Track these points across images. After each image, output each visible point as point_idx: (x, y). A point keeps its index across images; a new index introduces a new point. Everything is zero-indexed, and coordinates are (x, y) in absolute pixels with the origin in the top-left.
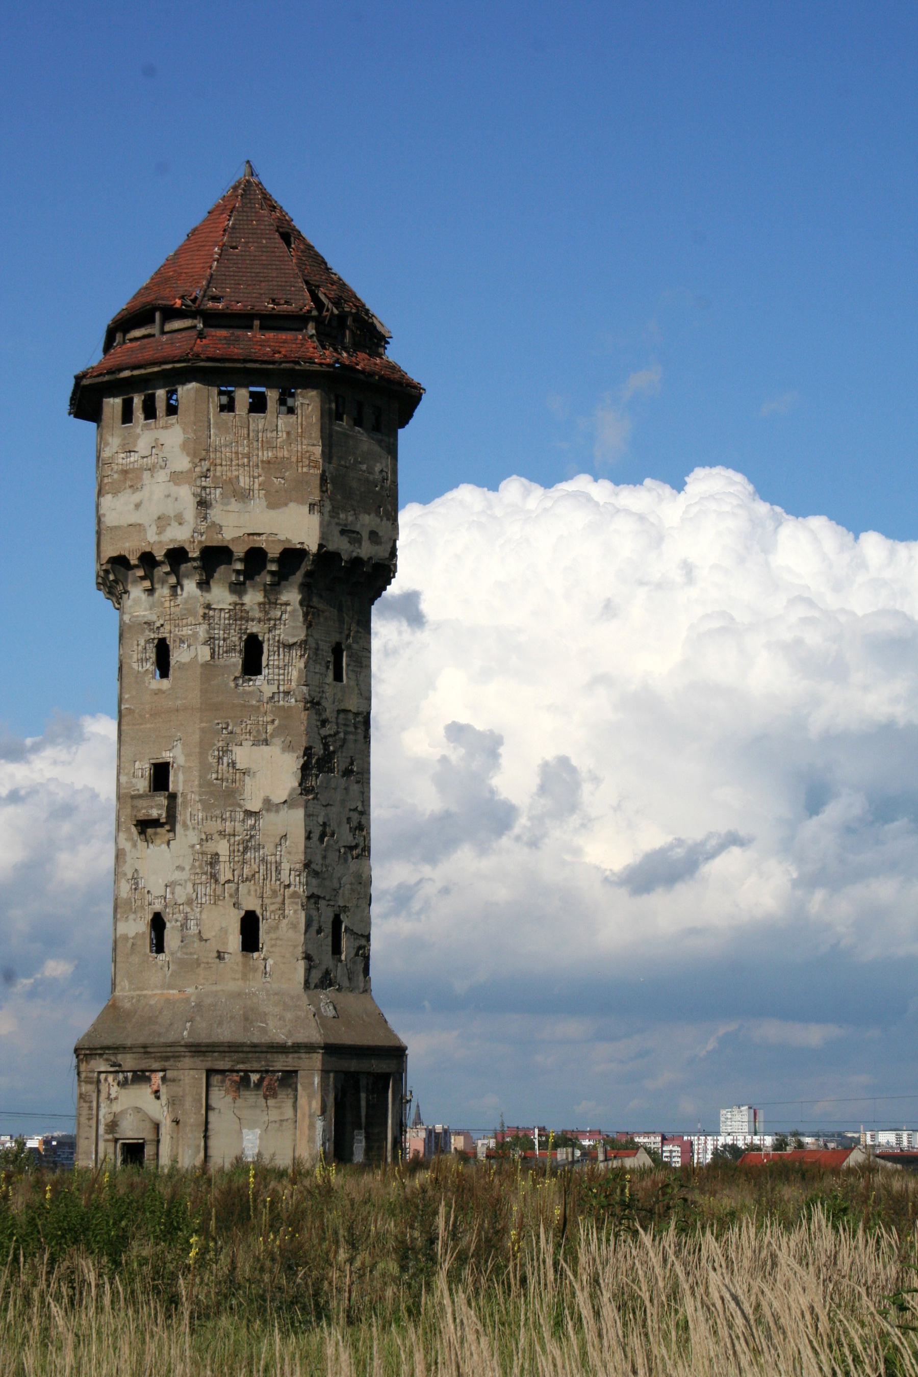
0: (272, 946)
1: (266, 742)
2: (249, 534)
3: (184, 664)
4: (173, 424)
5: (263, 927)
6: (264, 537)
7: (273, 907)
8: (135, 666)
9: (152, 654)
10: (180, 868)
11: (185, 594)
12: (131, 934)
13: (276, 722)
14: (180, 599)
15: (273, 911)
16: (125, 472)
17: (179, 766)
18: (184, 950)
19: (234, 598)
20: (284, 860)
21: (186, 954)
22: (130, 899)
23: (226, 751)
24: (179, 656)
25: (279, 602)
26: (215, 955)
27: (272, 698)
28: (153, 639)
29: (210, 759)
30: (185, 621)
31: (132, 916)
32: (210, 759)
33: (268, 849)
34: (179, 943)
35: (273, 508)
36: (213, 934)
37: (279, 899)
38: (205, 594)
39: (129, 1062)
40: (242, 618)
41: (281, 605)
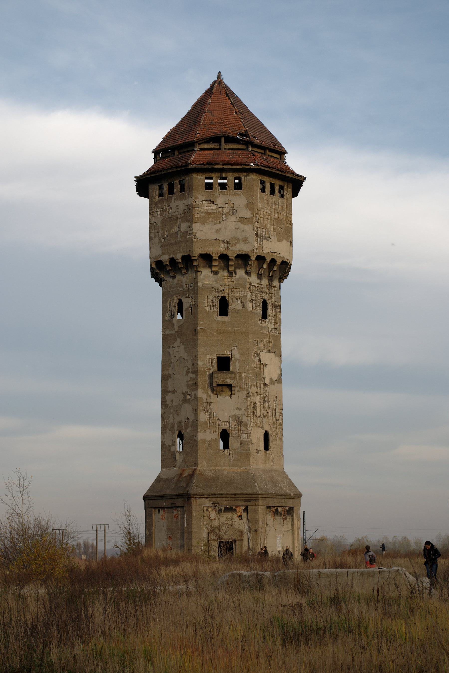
0: (274, 448)
1: (269, 351)
2: (271, 252)
4: (239, 194)
5: (271, 438)
6: (276, 254)
7: (274, 430)
8: (206, 308)
9: (217, 303)
11: (238, 276)
12: (208, 439)
13: (273, 342)
14: (234, 279)
15: (274, 432)
16: (209, 214)
17: (236, 360)
18: (242, 448)
19: (258, 281)
20: (277, 408)
21: (244, 450)
22: (206, 422)
23: (257, 354)
25: (273, 285)
26: (256, 451)
27: (271, 330)
28: (218, 296)
29: (252, 357)
30: (238, 290)
31: (208, 431)
32: (252, 357)
33: (272, 402)
34: (239, 445)
35: (279, 241)
36: (255, 441)
37: (275, 426)
38: (249, 278)
39: (224, 502)
40: (261, 291)
41: (273, 287)
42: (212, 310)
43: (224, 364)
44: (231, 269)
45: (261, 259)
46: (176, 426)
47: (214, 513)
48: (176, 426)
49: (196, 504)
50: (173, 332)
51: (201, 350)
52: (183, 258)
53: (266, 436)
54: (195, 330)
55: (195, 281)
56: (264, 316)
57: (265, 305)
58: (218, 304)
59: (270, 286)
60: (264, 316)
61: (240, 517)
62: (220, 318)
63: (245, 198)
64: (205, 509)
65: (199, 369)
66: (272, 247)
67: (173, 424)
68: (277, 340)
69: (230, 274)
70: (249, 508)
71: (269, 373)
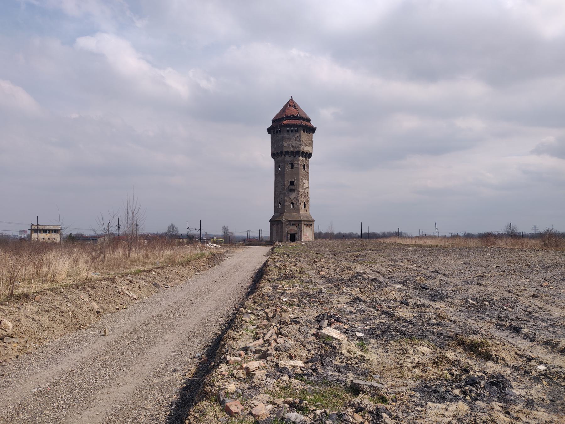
16: (288, 139)
24: (296, 166)
39: (292, 223)
43: (292, 183)
45: (303, 152)
51: (286, 179)
53: (305, 204)
56: (304, 169)
57: (304, 166)
59: (306, 160)
60: (304, 169)
66: (306, 149)
68: (308, 176)
71: (306, 185)
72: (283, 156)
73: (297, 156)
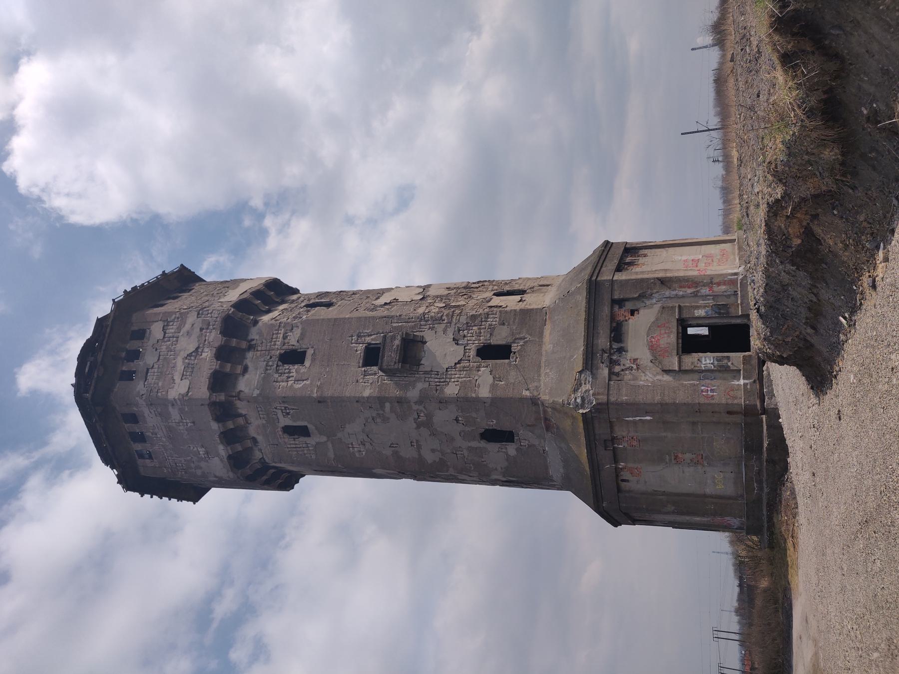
3: (301, 334)
10: (445, 331)
11: (257, 337)
21: (515, 319)
28: (277, 366)
39: (603, 341)
42: (294, 374)
43: (372, 356)
44: (244, 345)
46: (474, 444)
47: (622, 361)
48: (474, 444)
49: (603, 394)
50: (330, 445)
51: (349, 392)
52: (218, 419)
54: (319, 402)
55: (250, 400)
58: (286, 366)
61: (632, 313)
62: (307, 363)
63: (156, 324)
64: (614, 377)
65: (375, 394)
67: (470, 449)
69: (251, 347)
70: (616, 297)
72: (242, 407)
73: (254, 334)
